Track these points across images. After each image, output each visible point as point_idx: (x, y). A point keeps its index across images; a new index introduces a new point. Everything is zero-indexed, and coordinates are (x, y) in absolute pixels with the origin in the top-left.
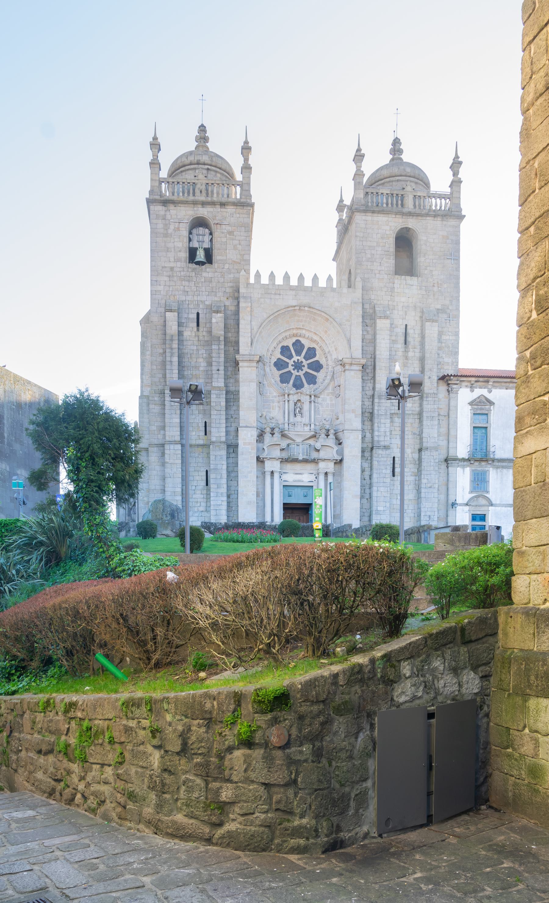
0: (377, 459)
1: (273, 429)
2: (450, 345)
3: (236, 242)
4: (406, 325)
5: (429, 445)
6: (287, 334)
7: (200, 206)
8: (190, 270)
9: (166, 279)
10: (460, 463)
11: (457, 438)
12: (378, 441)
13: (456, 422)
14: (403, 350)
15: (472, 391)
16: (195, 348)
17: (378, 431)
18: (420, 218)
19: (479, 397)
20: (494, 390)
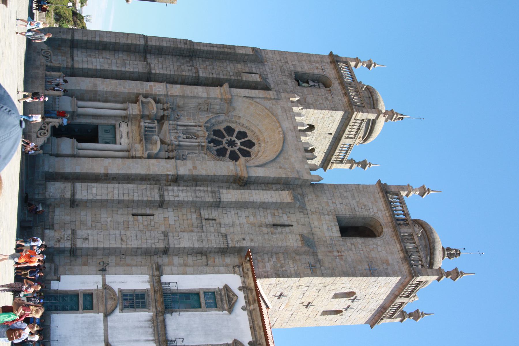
0: (148, 188)
1: (168, 109)
2: (284, 269)
3: (321, 102)
4: (292, 226)
5: (170, 238)
6: (258, 133)
7: (339, 81)
9: (278, 59)
11: (183, 274)
12: (167, 190)
13: (201, 273)
14: (268, 223)
15: (240, 289)
17: (178, 190)
18: (395, 237)
19: (234, 295)
20: (245, 314)
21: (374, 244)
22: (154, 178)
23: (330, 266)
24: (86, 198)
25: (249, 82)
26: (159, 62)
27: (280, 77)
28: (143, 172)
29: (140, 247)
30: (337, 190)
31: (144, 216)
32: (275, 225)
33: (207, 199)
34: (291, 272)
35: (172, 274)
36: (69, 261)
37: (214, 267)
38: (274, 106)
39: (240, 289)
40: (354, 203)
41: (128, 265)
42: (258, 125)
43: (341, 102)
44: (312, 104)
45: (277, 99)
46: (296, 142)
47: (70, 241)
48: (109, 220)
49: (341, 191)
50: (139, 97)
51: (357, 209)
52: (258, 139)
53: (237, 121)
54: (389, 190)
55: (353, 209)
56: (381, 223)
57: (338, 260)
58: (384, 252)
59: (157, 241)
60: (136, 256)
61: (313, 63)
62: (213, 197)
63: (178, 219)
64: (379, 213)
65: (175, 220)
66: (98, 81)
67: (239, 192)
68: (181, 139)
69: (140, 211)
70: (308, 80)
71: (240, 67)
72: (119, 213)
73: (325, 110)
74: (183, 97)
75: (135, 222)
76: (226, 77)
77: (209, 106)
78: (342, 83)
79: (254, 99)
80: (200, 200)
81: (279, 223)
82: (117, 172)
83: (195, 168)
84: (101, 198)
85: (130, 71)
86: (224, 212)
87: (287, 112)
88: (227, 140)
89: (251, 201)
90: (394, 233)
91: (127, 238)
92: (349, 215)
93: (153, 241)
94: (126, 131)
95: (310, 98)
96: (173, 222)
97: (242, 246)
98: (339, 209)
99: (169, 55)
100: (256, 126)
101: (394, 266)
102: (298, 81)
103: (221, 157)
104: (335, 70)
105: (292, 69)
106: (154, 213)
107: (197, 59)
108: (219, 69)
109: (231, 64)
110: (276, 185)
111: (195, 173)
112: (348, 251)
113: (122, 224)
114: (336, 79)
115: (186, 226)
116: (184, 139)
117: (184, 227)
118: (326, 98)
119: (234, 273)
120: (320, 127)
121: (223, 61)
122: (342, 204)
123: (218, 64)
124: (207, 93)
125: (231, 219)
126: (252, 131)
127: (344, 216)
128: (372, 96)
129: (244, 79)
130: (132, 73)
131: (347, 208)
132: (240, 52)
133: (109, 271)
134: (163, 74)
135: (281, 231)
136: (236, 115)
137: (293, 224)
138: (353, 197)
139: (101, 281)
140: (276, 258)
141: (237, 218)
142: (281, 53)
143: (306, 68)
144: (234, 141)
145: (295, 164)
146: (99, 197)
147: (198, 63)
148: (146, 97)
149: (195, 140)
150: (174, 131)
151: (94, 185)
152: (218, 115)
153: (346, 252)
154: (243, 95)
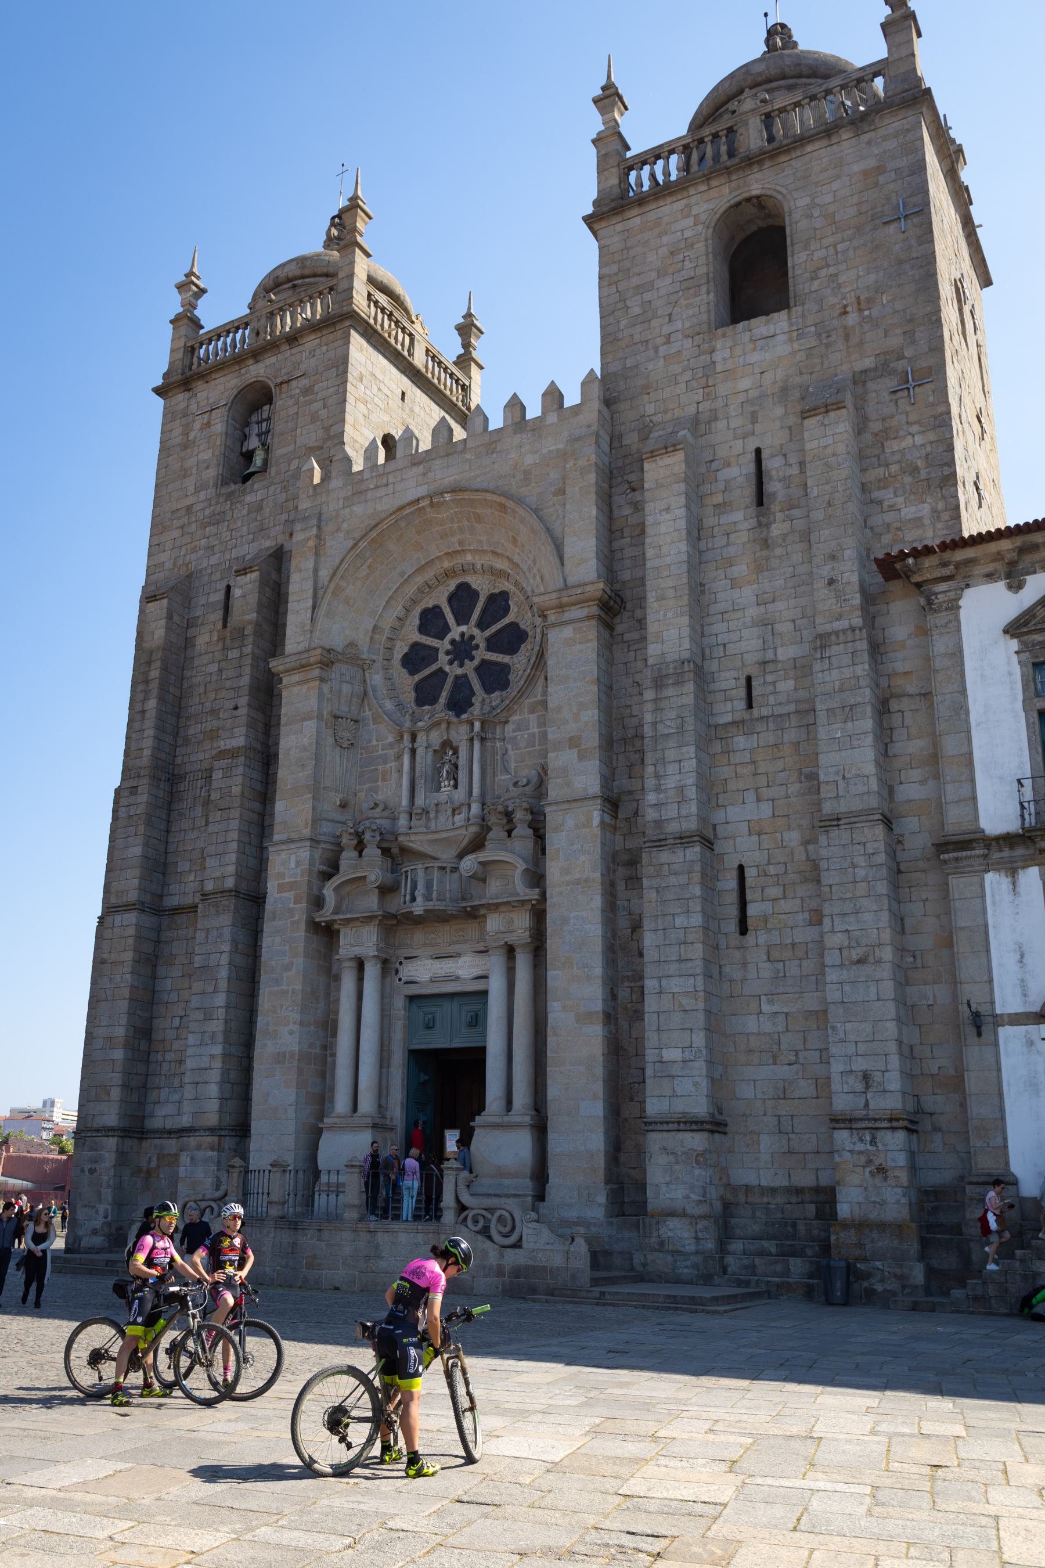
1: (359, 836)
2: (920, 463)
3: (318, 405)
4: (758, 452)
5: (843, 807)
6: (429, 575)
8: (221, 500)
10: (996, 855)
11: (970, 764)
12: (659, 823)
13: (961, 709)
14: (753, 522)
15: (1016, 586)
16: (213, 668)
17: (658, 789)
18: (783, 158)
21: (810, 216)
22: (608, 868)
23: (898, 331)
24: (704, 1084)
25: (260, 605)
26: (190, 871)
27: (239, 524)
28: (597, 901)
29: (886, 901)
30: (620, 335)
31: (749, 896)
32: (760, 499)
33: (689, 700)
34: (932, 443)
35: (974, 798)
36: (938, 1137)
37: (936, 671)
38: (345, 526)
39: (1016, 586)
40: (665, 285)
41: (948, 941)
42: (402, 574)
43: (318, 352)
44: (327, 429)
45: (320, 520)
46: (468, 456)
47: (880, 1134)
48: (766, 1008)
49: (624, 323)
50: (319, 923)
51: (685, 274)
52: (449, 574)
53: (387, 633)
54: (617, 191)
55: (686, 284)
56: (732, 202)
57: (875, 312)
58: (836, 185)
59: (861, 847)
60: (902, 920)
61: (191, 438)
62: (678, 683)
63: (752, 792)
64: (695, 211)
65: (759, 800)
66: (264, 1050)
67: (656, 605)
68: (460, 795)
69: (733, 911)
70: (242, 454)
71: (205, 638)
72: (737, 975)
73: (345, 391)
74: (316, 790)
75: (769, 926)
76: (247, 670)
77: (343, 714)
78: (256, 354)
79: (320, 585)
80: (690, 721)
81: (750, 491)
82: (599, 981)
83: (573, 742)
84: (702, 1034)
85: (231, 952)
86: (719, 652)
87: (363, 487)
88: (451, 663)
89: (685, 567)
90: (767, 164)
91: (854, 944)
92: (708, 293)
93: (861, 861)
94: (431, 961)
95: (309, 435)
96: (766, 809)
97: (857, 587)
98: (687, 324)
99: (167, 843)
100: (406, 580)
101: (884, 152)
102: (246, 479)
103: (511, 677)
104: (213, 376)
105: (211, 492)
106: (736, 866)
107: (179, 760)
108: (212, 696)
109: (196, 663)
110: (614, 507)
111: (592, 739)
112: (839, 286)
113: (780, 966)
114: (243, 371)
115: (780, 764)
116: (456, 787)
117: (784, 770)
118: (307, 391)
119: (954, 607)
120: (386, 418)
121: (185, 686)
122: (670, 315)
123: (196, 700)
124: (304, 719)
125: (746, 633)
126: (420, 591)
127: (712, 307)
128: (289, 280)
129: (254, 616)
130: (236, 946)
131: (683, 302)
132: (158, 633)
133: (979, 1004)
134: (239, 852)
135: (780, 481)
136: (368, 640)
137: (751, 448)
138: (649, 286)
139: (1020, 1030)
140: (879, 489)
141: (739, 614)
142: (158, 526)
143: (207, 455)
144: (453, 642)
145: (545, 451)
146: (699, 1039)
147: (193, 758)
148: (318, 902)
149: (463, 753)
150: (432, 815)
151: (650, 1055)
152: (370, 689)
153: (844, 290)
154: (309, 616)
